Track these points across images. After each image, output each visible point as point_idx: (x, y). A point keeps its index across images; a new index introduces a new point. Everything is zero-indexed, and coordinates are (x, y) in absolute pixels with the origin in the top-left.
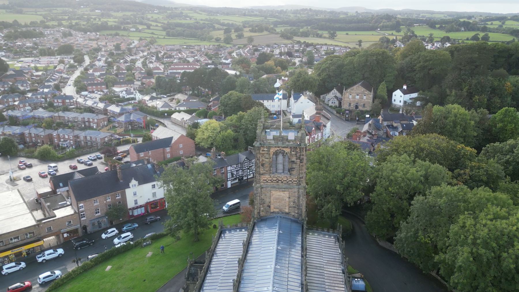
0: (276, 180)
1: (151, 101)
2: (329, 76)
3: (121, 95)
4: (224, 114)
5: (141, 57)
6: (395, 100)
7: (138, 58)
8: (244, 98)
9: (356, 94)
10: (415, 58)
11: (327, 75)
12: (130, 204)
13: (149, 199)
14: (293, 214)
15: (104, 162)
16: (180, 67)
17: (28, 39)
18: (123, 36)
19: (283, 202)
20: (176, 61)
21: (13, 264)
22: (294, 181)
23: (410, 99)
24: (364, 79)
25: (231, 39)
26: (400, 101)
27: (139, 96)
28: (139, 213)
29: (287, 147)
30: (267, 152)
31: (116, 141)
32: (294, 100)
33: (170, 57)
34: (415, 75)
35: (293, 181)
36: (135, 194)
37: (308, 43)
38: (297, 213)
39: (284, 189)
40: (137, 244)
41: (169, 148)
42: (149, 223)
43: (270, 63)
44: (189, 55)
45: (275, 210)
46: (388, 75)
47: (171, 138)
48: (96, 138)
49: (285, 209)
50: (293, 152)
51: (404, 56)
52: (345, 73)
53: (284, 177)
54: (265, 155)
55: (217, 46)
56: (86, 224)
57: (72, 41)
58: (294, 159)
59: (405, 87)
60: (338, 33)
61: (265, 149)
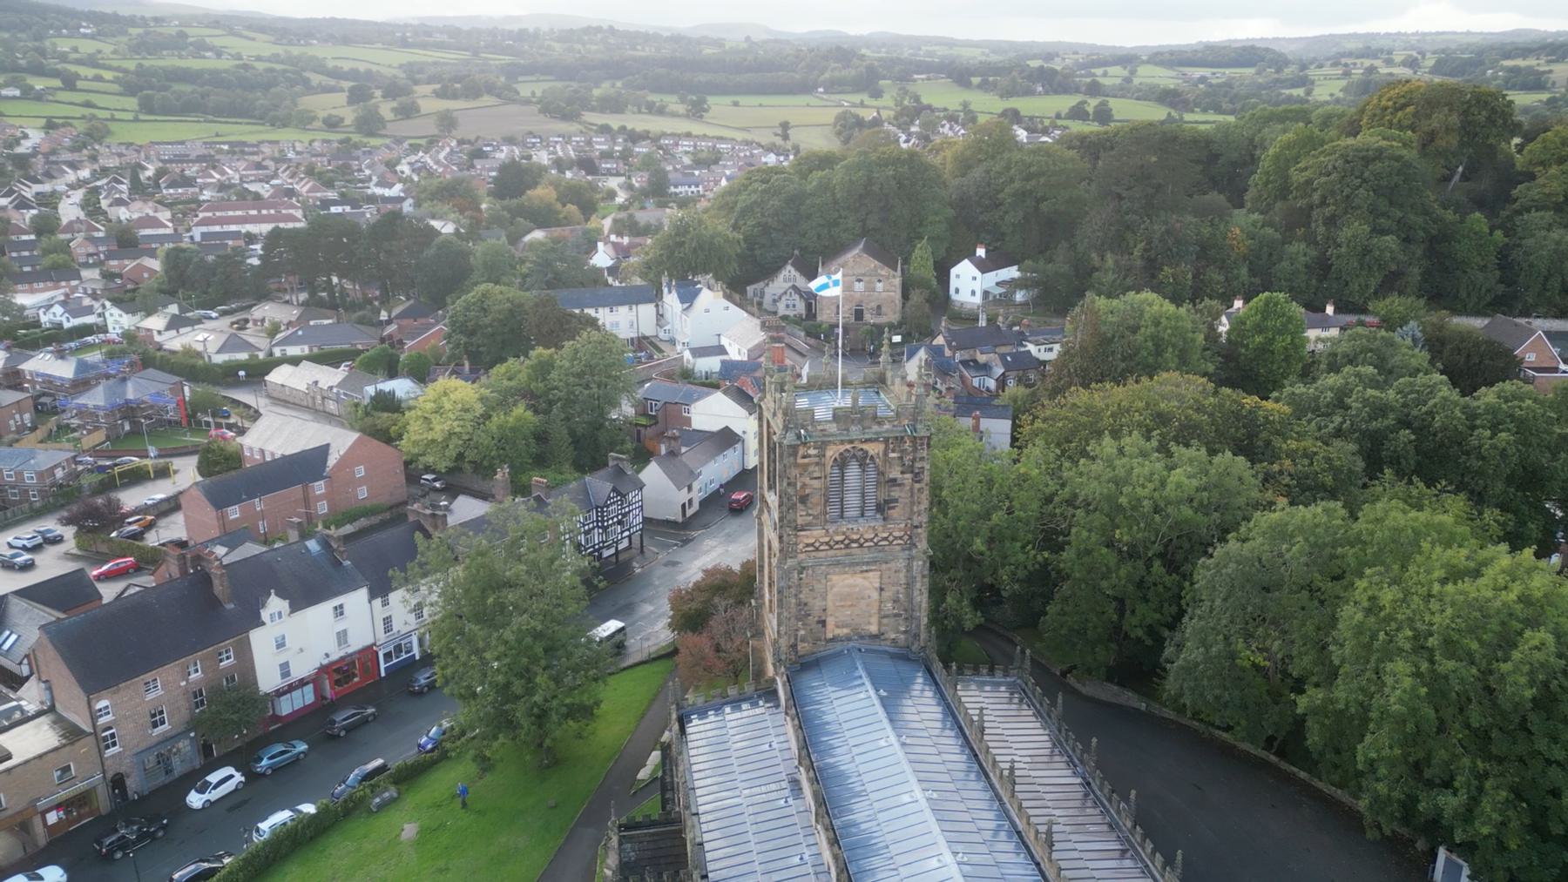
0: (842, 542)
1: (173, 333)
2: (766, 229)
3: (44, 319)
4: (468, 359)
5: (72, 187)
6: (957, 291)
7: (61, 188)
8: (537, 305)
9: (854, 278)
10: (998, 168)
11: (759, 224)
12: (268, 679)
13: (327, 655)
14: (893, 636)
15: (75, 551)
16: (231, 213)
19: (863, 603)
20: (207, 195)
22: (896, 538)
23: (998, 284)
24: (865, 232)
25: (382, 122)
26: (973, 293)
27: (118, 321)
28: (298, 705)
29: (876, 440)
30: (816, 459)
31: (96, 478)
32: (682, 302)
33: (188, 182)
34: (1002, 218)
35: (891, 538)
36: (281, 644)
37: (633, 130)
38: (905, 632)
39: (868, 563)
40: (351, 805)
41: (322, 482)
42: (343, 734)
43: (541, 193)
44: (247, 176)
45: (838, 632)
46: (930, 219)
47: (324, 450)
48: (19, 474)
49: (869, 623)
50: (893, 451)
51: (964, 165)
52: (809, 217)
53: (865, 528)
54: (811, 469)
55: (341, 142)
56: (123, 769)
58: (895, 473)
59: (981, 252)
60: (711, 100)
61: (812, 452)
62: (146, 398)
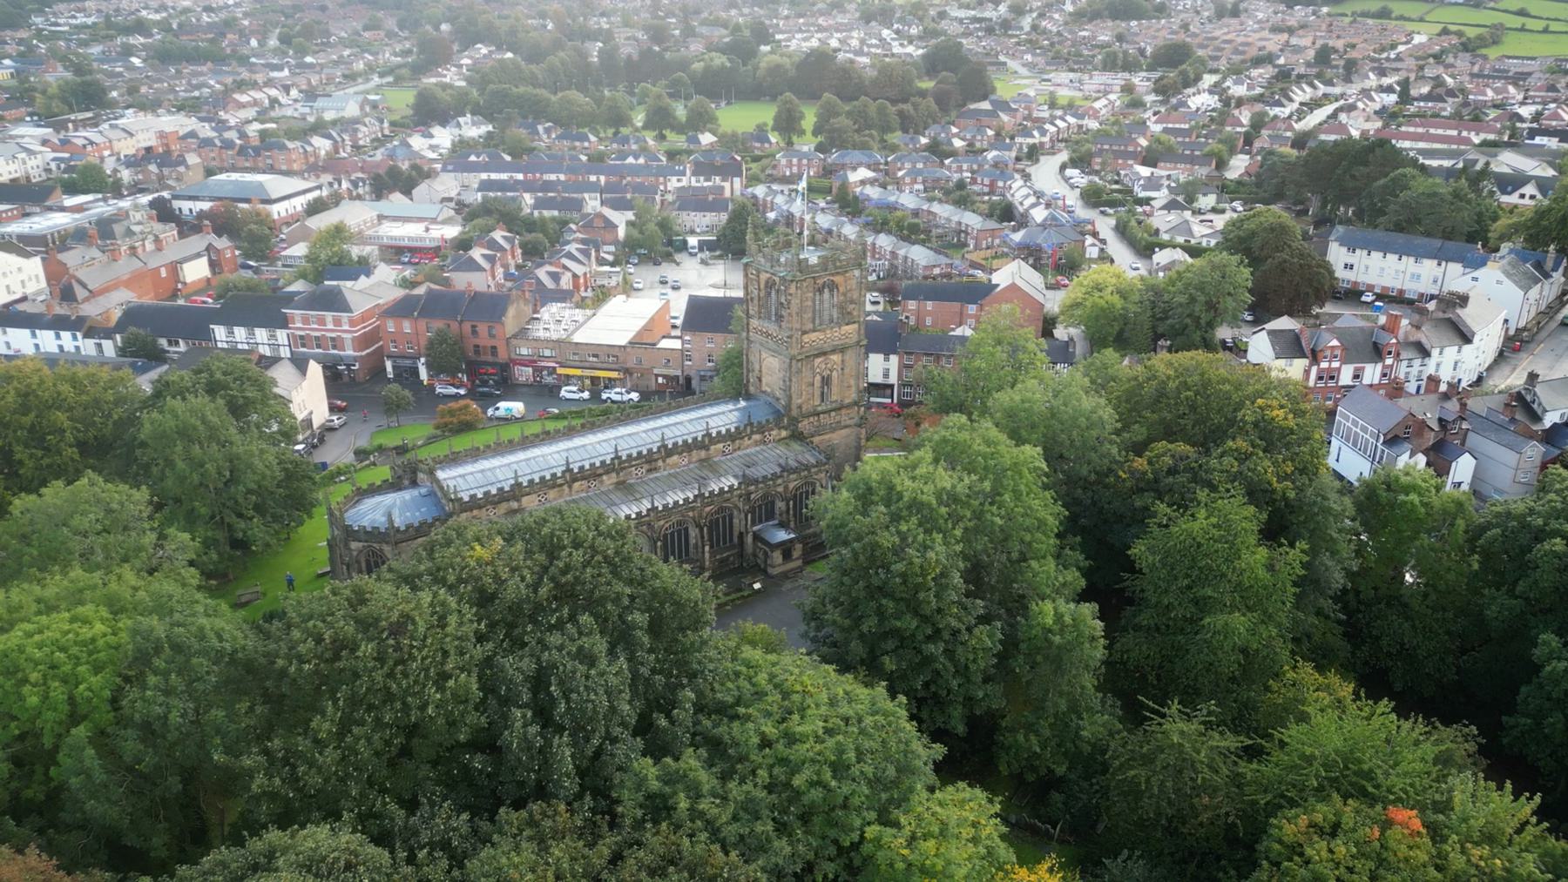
17: (1118, 22)
18: (1402, 18)
21: (575, 389)
44: (1532, 97)
47: (998, 285)
57: (1217, 33)
58: (783, 300)
62: (1044, 245)
